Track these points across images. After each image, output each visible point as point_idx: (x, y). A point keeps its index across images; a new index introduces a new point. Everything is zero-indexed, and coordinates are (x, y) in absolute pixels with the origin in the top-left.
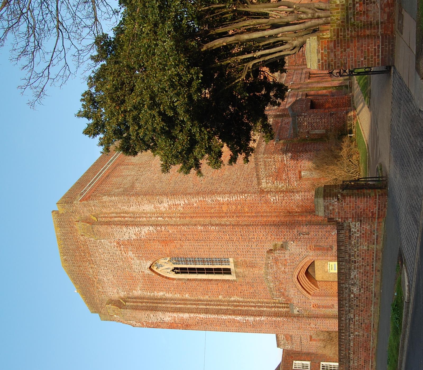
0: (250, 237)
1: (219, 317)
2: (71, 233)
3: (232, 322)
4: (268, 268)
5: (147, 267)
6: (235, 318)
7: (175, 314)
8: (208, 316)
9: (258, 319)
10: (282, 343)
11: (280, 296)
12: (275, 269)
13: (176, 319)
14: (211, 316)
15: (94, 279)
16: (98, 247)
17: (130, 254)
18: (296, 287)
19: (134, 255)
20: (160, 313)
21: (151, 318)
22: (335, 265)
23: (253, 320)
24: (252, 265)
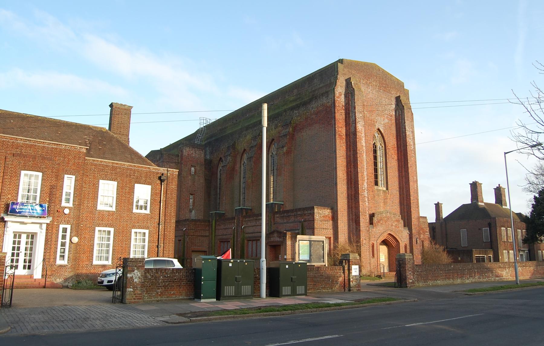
0: (413, 208)
1: (365, 169)
2: (395, 87)
3: (362, 178)
4: (394, 214)
5: (380, 127)
6: (365, 182)
7: (364, 135)
8: (365, 161)
9: (366, 199)
10: (320, 212)
11: (377, 219)
12: (393, 219)
13: (361, 134)
14: (365, 164)
15: (369, 82)
16: (389, 100)
17: (386, 121)
18: (384, 232)
19: (386, 123)
20: (364, 124)
21: (359, 114)
22: (383, 259)
23: (365, 195)
24: (385, 203)
